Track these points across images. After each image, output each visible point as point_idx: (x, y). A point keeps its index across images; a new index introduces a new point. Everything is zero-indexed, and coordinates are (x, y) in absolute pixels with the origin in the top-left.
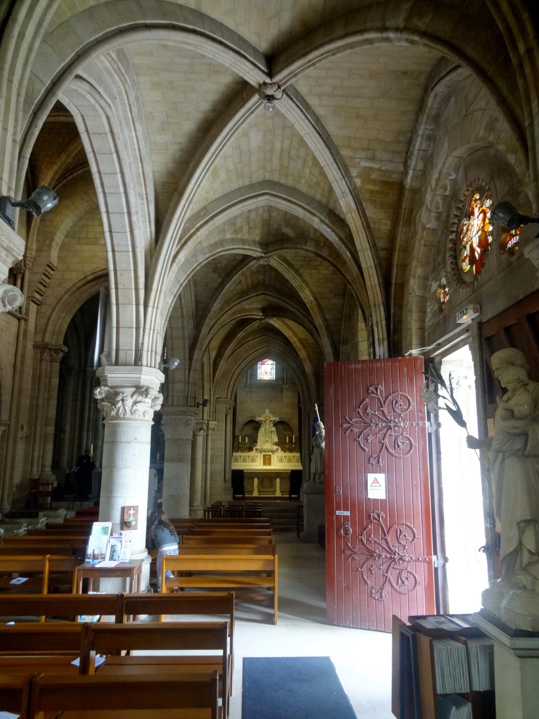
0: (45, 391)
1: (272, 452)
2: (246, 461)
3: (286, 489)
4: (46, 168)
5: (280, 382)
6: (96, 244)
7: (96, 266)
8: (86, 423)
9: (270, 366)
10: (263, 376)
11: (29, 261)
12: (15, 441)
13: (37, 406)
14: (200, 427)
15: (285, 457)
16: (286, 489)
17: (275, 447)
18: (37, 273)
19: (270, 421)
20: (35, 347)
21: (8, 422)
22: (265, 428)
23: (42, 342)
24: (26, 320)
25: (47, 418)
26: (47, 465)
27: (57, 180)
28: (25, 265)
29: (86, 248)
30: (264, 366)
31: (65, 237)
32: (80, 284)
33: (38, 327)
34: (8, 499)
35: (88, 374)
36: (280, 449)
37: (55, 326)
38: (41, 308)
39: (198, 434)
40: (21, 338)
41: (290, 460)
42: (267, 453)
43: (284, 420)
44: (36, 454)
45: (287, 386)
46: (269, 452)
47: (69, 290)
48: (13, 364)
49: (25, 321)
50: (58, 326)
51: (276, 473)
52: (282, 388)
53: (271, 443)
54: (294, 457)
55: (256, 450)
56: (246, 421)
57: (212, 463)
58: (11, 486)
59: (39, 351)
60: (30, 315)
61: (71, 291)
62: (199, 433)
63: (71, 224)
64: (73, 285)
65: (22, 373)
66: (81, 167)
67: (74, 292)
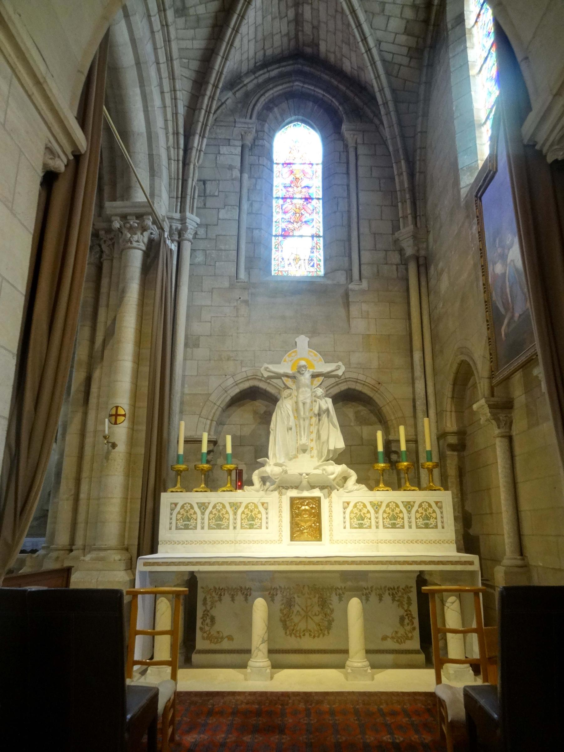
1: (322, 488)
2: (224, 522)
3: (385, 638)
5: (341, 278)
9: (309, 242)
10: (287, 268)
15: (376, 506)
16: (385, 638)
17: (337, 469)
19: (314, 376)
22: (297, 403)
30: (289, 239)
36: (354, 476)
42: (306, 494)
43: (359, 387)
45: (365, 284)
46: (312, 487)
51: (345, 575)
52: (346, 295)
53: (320, 455)
54: (409, 505)
55: (264, 480)
56: (236, 390)
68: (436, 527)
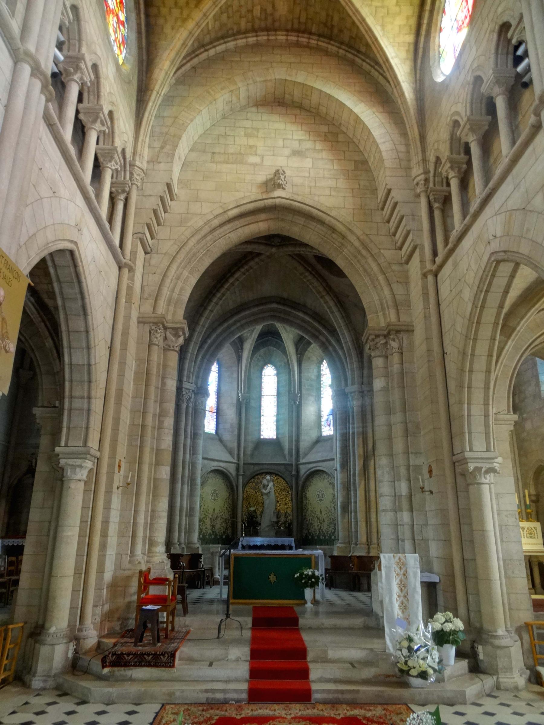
0: (156, 401)
4: (173, 28)
6: (242, 163)
7: (241, 195)
8: (180, 469)
11: (138, 175)
12: (109, 492)
13: (143, 427)
14: (488, 466)
18: (151, 196)
20: (141, 321)
21: (98, 454)
23: (154, 312)
24: (131, 270)
25: (159, 451)
26: (159, 541)
27: (184, 58)
28: (131, 179)
29: (225, 167)
31: (190, 151)
32: (216, 222)
33: (146, 288)
34: (93, 615)
35: (184, 393)
37: (173, 291)
38: (150, 258)
39: (483, 480)
40: (123, 300)
41: (531, 534)
44: (141, 519)
47: (197, 231)
48: (109, 345)
49: (129, 271)
50: (177, 291)
57: (502, 541)
58: (99, 588)
59: (147, 328)
60: (137, 263)
61: (203, 233)
62: (485, 478)
63: (200, 131)
64: (205, 224)
65: (123, 364)
66: (222, 41)
67: (205, 236)
68: (535, 538)
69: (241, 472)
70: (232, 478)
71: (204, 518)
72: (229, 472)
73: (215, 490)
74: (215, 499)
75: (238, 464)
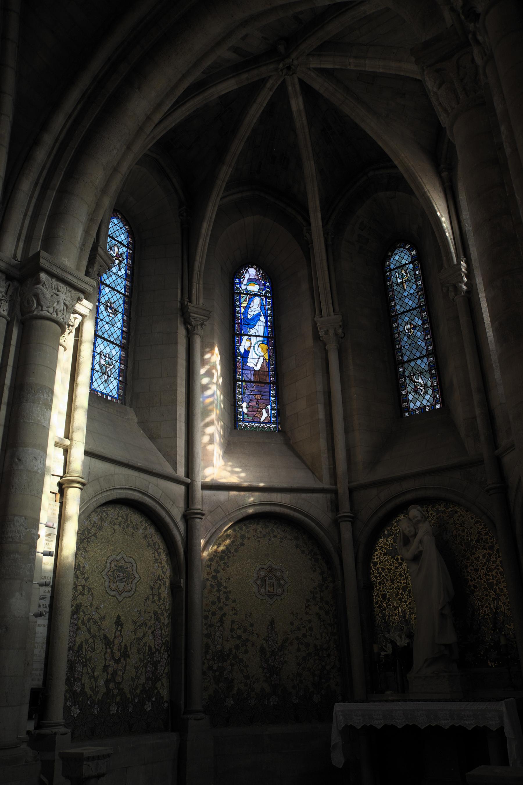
69: (345, 510)
70: (322, 533)
71: (237, 647)
72: (306, 516)
73: (270, 569)
74: (271, 595)
75: (335, 492)
